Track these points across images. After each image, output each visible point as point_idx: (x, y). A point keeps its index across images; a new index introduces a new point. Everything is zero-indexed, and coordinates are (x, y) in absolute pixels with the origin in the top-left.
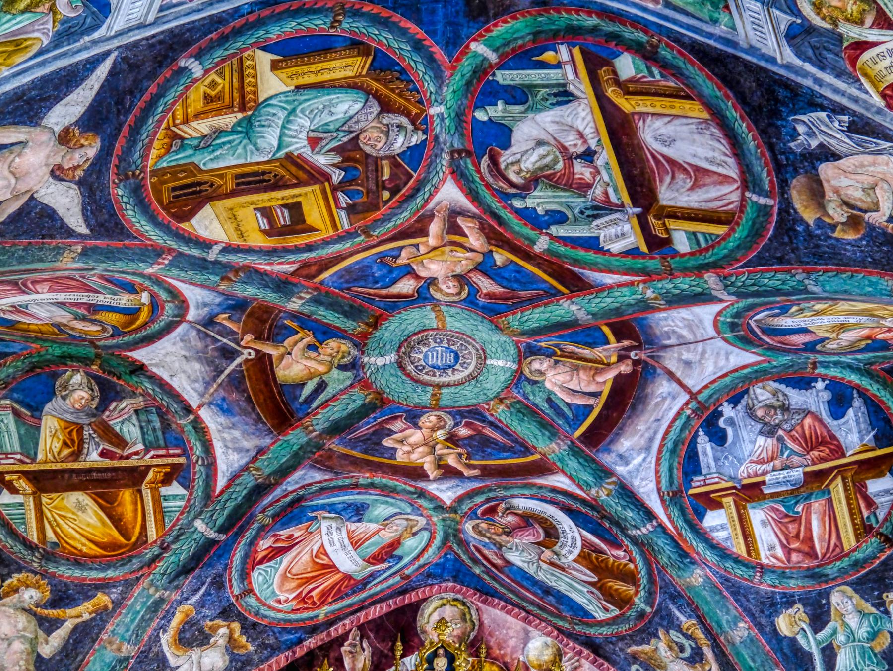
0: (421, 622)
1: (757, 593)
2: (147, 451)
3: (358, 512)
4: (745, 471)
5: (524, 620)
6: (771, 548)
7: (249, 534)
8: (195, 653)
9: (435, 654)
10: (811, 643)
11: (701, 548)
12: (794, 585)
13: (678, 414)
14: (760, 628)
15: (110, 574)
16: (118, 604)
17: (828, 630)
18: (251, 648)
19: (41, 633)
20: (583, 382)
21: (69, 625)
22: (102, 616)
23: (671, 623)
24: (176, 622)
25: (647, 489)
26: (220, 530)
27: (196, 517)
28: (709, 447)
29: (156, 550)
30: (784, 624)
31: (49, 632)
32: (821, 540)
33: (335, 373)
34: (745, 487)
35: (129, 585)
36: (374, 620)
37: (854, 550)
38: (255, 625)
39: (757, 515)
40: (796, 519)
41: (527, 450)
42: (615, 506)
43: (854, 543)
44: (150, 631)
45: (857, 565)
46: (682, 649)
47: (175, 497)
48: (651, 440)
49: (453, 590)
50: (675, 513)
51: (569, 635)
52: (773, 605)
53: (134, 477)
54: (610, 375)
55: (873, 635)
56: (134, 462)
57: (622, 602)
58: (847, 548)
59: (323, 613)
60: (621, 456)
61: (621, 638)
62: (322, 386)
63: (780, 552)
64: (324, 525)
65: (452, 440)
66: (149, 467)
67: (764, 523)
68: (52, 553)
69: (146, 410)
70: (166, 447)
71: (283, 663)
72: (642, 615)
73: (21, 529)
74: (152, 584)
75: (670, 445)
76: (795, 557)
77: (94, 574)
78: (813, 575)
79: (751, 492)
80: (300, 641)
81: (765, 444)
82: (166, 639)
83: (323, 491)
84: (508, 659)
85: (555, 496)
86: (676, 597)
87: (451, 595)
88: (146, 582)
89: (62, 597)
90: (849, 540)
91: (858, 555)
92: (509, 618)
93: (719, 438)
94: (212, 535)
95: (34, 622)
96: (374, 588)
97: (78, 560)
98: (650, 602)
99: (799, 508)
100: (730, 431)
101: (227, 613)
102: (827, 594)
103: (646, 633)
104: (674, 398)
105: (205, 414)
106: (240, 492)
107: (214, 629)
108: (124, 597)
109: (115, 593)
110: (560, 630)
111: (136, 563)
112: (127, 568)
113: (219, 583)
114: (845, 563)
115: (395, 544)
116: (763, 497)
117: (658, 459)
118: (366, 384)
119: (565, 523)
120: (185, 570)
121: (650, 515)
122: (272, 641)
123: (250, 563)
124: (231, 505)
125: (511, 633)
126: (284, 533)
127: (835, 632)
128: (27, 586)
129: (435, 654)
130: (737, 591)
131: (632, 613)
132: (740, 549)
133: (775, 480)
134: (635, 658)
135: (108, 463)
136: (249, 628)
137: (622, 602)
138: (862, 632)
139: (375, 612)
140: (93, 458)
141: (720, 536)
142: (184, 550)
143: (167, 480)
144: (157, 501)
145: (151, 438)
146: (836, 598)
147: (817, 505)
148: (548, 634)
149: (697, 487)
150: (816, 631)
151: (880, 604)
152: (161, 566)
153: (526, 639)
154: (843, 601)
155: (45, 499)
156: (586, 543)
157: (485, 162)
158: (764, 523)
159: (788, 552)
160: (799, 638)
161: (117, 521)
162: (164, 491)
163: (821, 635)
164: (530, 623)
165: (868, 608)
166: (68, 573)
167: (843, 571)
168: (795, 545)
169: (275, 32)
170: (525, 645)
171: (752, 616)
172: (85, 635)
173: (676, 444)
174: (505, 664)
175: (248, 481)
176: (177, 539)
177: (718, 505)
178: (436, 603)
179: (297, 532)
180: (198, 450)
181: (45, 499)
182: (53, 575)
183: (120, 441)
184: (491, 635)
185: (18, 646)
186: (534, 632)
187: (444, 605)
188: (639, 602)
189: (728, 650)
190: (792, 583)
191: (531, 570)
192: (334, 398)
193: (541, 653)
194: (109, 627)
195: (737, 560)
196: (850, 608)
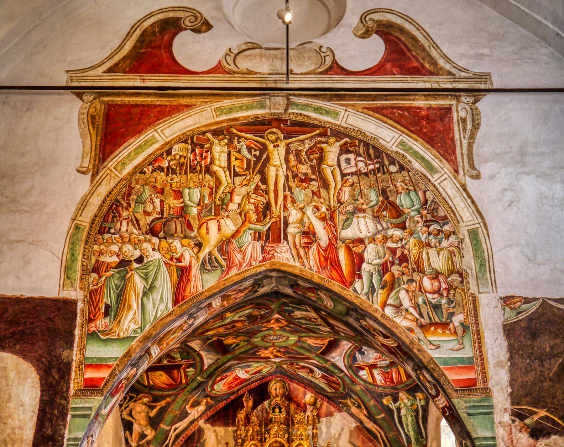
0: (269, 389)
1: (377, 392)
2: (182, 360)
3: (249, 366)
4: (371, 361)
5: (304, 387)
6: (380, 381)
7: (214, 378)
8: (196, 409)
9: (275, 408)
10: (393, 407)
11: (358, 380)
12: (387, 390)
13: (349, 348)
14: (378, 402)
15: (171, 392)
16: (173, 401)
17: (398, 403)
18: (213, 403)
19: (150, 410)
20: (319, 342)
21: (158, 407)
22: (169, 404)
23: (351, 397)
24: (190, 402)
25: (341, 365)
26: (206, 378)
27: (198, 376)
28: (359, 356)
29: (185, 385)
30: (385, 401)
31: (152, 410)
32: (396, 379)
33: (242, 342)
34: (371, 365)
35: (177, 395)
36: (253, 389)
37: (406, 382)
38: (214, 397)
39: (376, 372)
40: (388, 373)
41: (303, 355)
42: (331, 368)
43: (406, 380)
44: (183, 406)
45: (407, 386)
46: (355, 404)
47: (191, 371)
48: (341, 354)
49: (280, 377)
50: (350, 371)
51: (320, 393)
52: (382, 396)
53: (178, 367)
54: (328, 340)
55: (412, 405)
56: (178, 363)
57: (336, 389)
58: (404, 381)
59: (236, 389)
60: (332, 357)
61: (336, 397)
62: (238, 345)
63: (383, 382)
64: (237, 371)
65: (278, 351)
66: (182, 364)
67: (378, 374)
68: (152, 388)
69: (183, 352)
70: (188, 359)
71: (223, 405)
72: (342, 393)
73: (142, 382)
74: (184, 394)
75: (347, 355)
76: (388, 383)
77: (166, 393)
78: (393, 388)
79: (374, 366)
80: (228, 398)
81: (377, 355)
82: (187, 407)
83: (237, 364)
84: (299, 402)
85: (312, 364)
86: (352, 391)
87: (279, 379)
88: (182, 394)
89: (156, 400)
90: (404, 379)
91: (407, 383)
92: (299, 387)
93: (363, 354)
94: (203, 380)
95: (147, 408)
96: (252, 380)
97: (160, 389)
98: (344, 390)
99: (389, 370)
100: (366, 352)
101: (206, 396)
102: (398, 393)
103: (344, 397)
104: (348, 345)
105: (201, 352)
106: (211, 369)
107: (202, 401)
108: (175, 398)
109: (173, 398)
110: (316, 391)
111: (179, 389)
112: (176, 391)
113: (204, 390)
114: (403, 385)
115: (261, 370)
116: (377, 367)
117: (344, 358)
118: (251, 344)
119: (316, 369)
120: (194, 390)
121: (342, 371)
122: (219, 399)
123: (214, 383)
124: (208, 373)
125: (300, 392)
126: (224, 375)
127: (400, 404)
128: (145, 397)
129: (275, 408)
130: (370, 392)
131: (339, 392)
132: (371, 380)
133: (380, 364)
134: (341, 403)
135: (169, 364)
136: (212, 398)
137: (336, 389)
138: (409, 404)
139: (253, 385)
140: (165, 362)
141: (364, 377)
142: (194, 385)
143: (188, 367)
144: (185, 372)
145: (183, 357)
146: (400, 395)
147: (394, 370)
148: (312, 393)
149: (357, 364)
150: (395, 403)
151: (414, 396)
152: (187, 389)
153: (305, 394)
154: (402, 395)
155: (149, 374)
156: (322, 374)
157: (287, 314)
158: (378, 374)
159: (386, 382)
160: (390, 405)
161: (172, 378)
162: (187, 370)
163: (396, 405)
164: (306, 389)
165: (410, 397)
166: (157, 393)
167: (402, 387)
168: (388, 380)
169: (231, 310)
170: (305, 396)
171: (375, 399)
172: (163, 410)
173: (349, 355)
174: (298, 404)
175: (214, 367)
176: (192, 382)
177: (363, 369)
178: (274, 382)
179: (228, 374)
180: (198, 359)
181: (149, 374)
182: (152, 394)
183: (174, 358)
184: (293, 393)
185: (143, 414)
186: (308, 392)
187: (276, 383)
188: (341, 389)
189: (368, 407)
190: (387, 390)
191: (306, 377)
192: (241, 347)
193: (310, 400)
194: (171, 407)
195: (370, 384)
196: (405, 397)
